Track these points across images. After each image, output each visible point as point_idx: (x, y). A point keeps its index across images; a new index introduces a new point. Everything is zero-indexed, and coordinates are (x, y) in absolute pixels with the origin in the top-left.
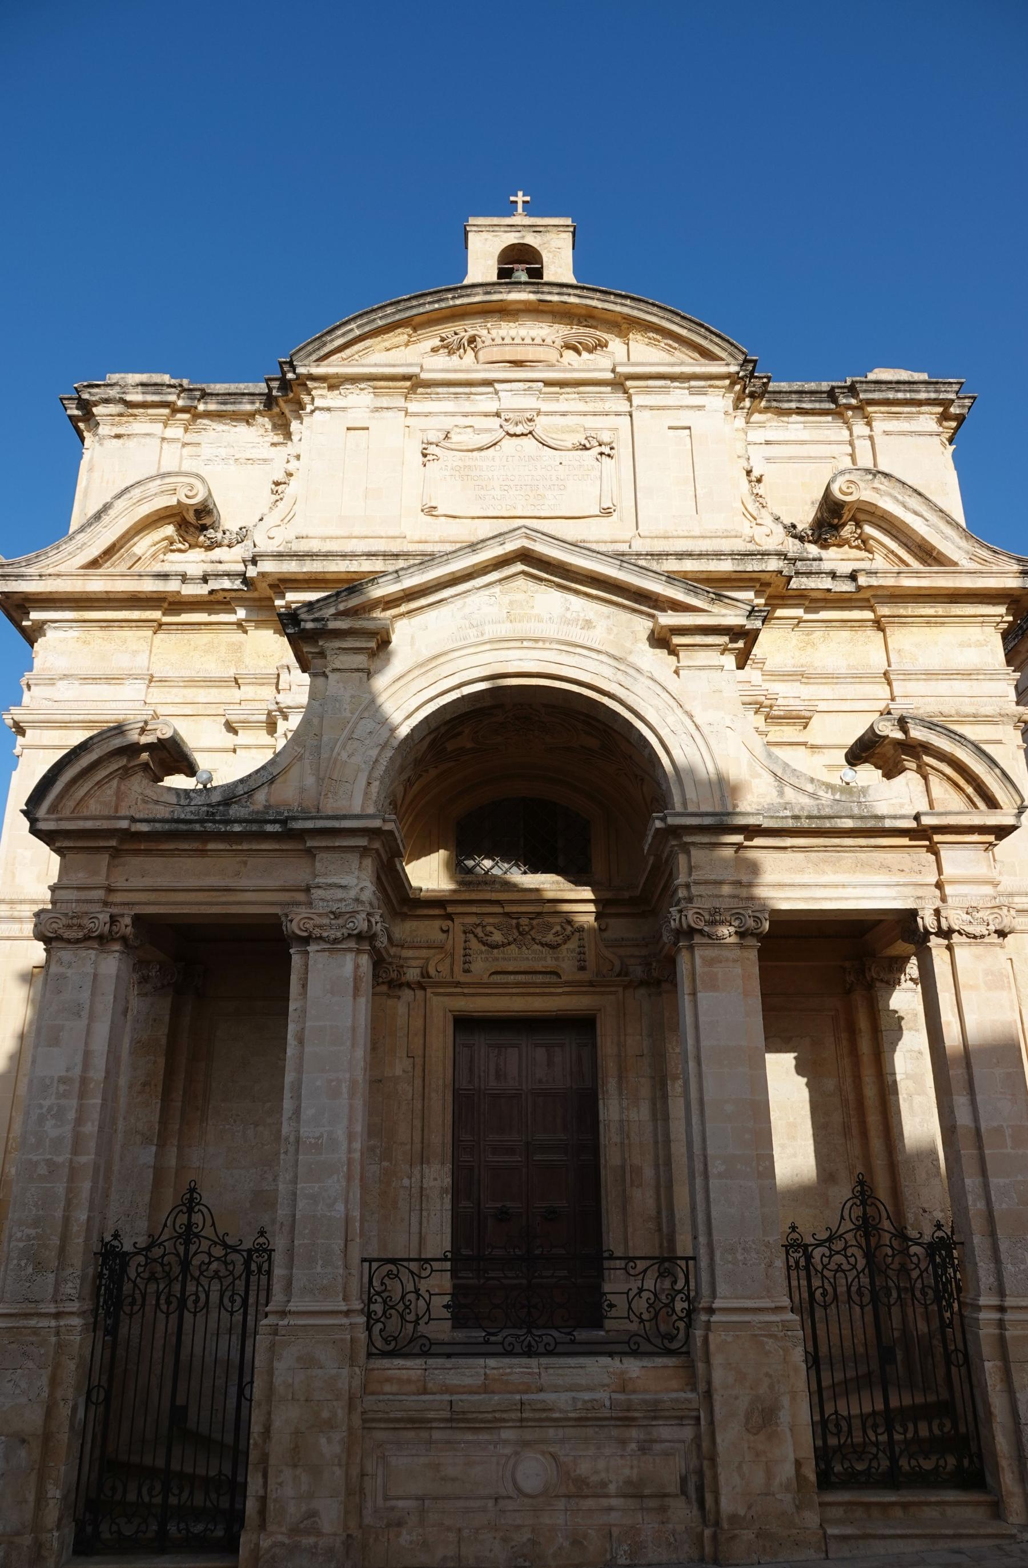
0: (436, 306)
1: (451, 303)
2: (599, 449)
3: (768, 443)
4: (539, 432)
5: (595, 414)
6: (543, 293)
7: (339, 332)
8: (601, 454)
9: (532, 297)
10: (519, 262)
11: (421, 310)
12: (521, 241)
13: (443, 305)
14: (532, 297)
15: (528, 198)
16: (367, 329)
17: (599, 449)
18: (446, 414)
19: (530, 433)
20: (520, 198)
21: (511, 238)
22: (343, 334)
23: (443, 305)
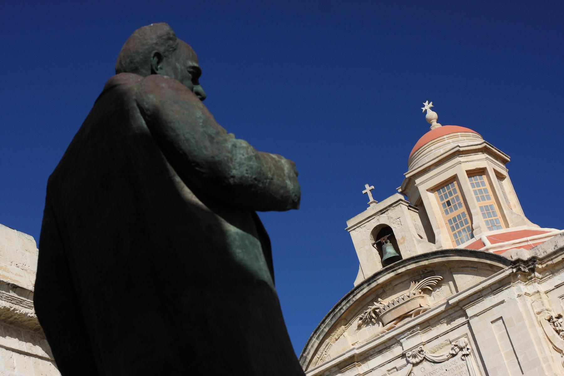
0: (348, 305)
1: (354, 299)
2: (461, 353)
3: (557, 287)
4: (429, 356)
5: (452, 330)
6: (395, 270)
7: (309, 347)
8: (464, 355)
9: (392, 274)
10: (383, 235)
11: (342, 311)
12: (378, 224)
13: (351, 302)
14: (392, 274)
15: (373, 187)
16: (321, 337)
17: (461, 353)
18: (380, 366)
19: (424, 358)
20: (368, 189)
21: (374, 223)
22: (312, 346)
23: (351, 302)
